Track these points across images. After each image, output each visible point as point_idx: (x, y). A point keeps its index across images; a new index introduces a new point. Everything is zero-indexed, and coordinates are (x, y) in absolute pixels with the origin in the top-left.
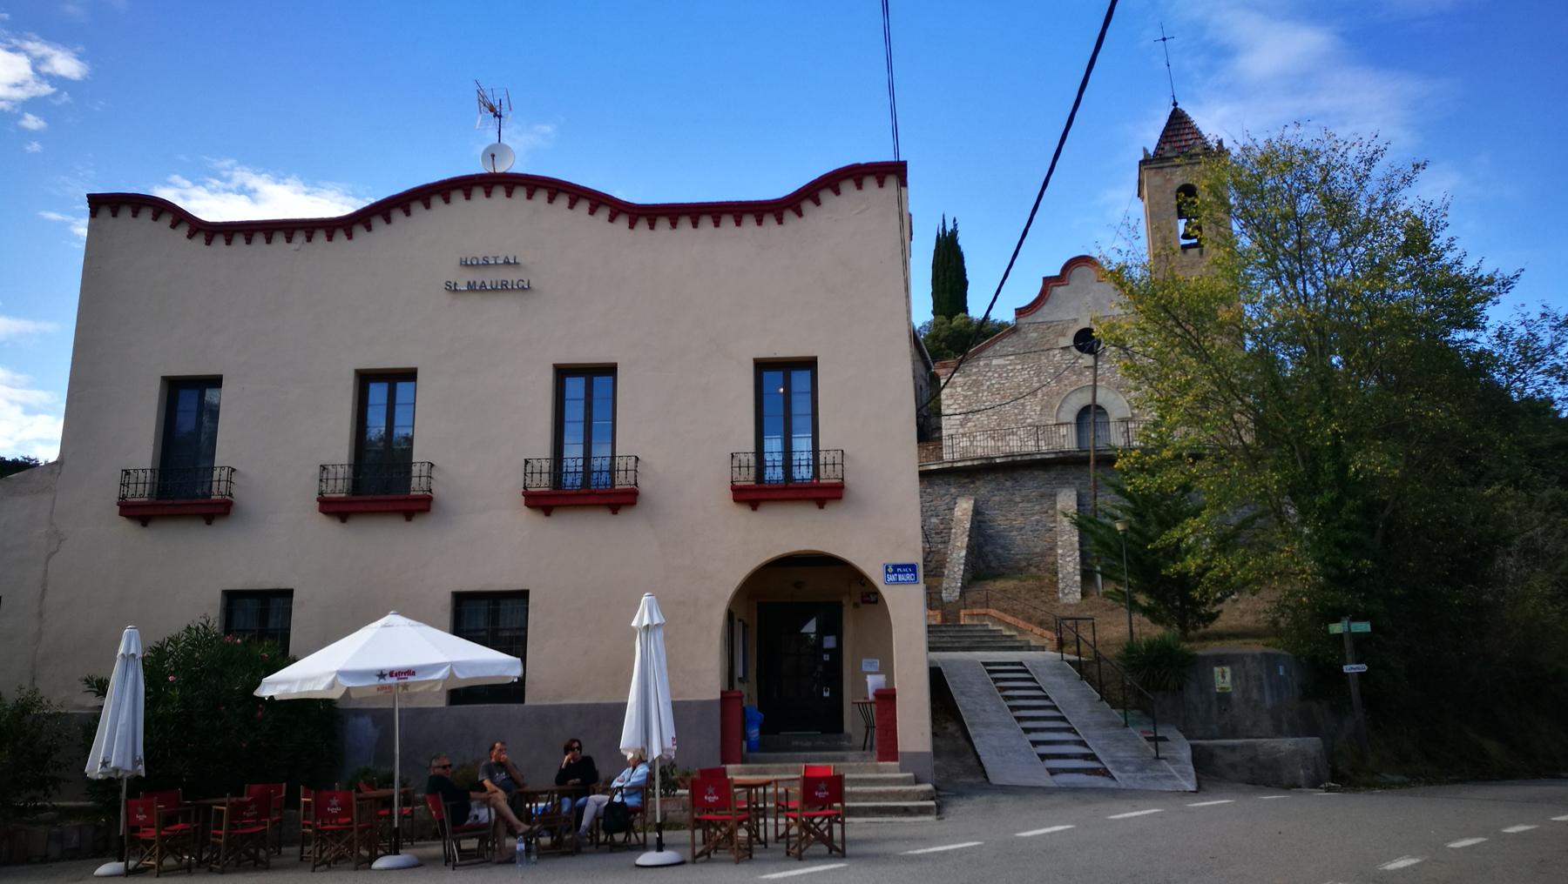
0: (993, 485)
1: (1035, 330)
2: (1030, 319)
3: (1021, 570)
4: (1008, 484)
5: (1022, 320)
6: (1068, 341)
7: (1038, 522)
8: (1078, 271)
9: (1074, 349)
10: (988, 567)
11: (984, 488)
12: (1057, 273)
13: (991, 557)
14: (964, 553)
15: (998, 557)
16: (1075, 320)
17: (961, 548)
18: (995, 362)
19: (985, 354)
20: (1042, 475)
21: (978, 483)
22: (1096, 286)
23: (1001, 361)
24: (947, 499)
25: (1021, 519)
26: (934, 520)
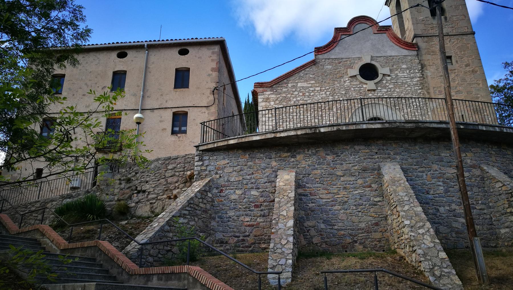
0: (314, 159)
1: (329, 64)
2: (326, 56)
3: (345, 248)
4: (329, 158)
5: (320, 57)
6: (355, 71)
7: (361, 196)
8: (359, 27)
9: (359, 77)
10: (310, 243)
11: (305, 160)
12: (345, 25)
13: (313, 232)
14: (291, 223)
15: (320, 232)
16: (360, 58)
17: (287, 218)
18: (299, 85)
19: (292, 78)
20: (363, 151)
21: (298, 157)
22: (373, 37)
23: (305, 85)
24: (268, 172)
25: (343, 193)
26: (254, 192)
